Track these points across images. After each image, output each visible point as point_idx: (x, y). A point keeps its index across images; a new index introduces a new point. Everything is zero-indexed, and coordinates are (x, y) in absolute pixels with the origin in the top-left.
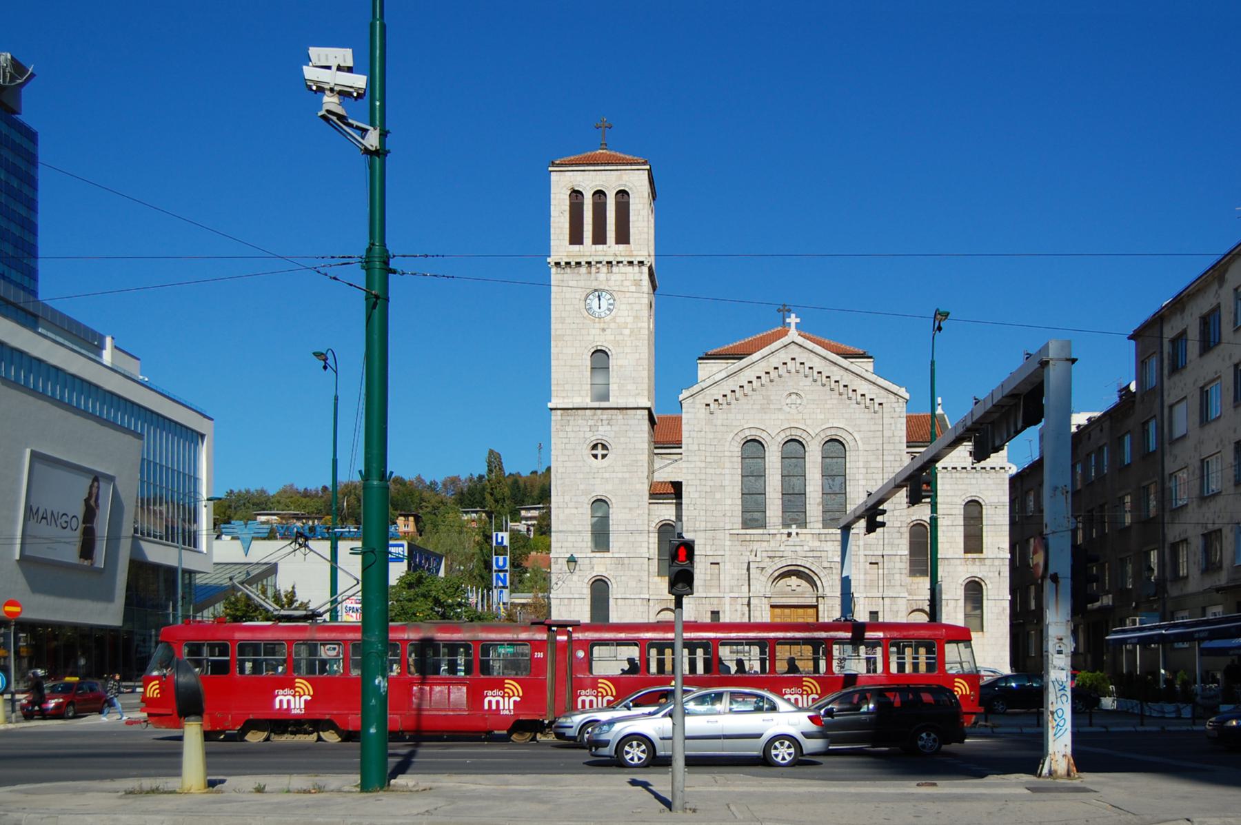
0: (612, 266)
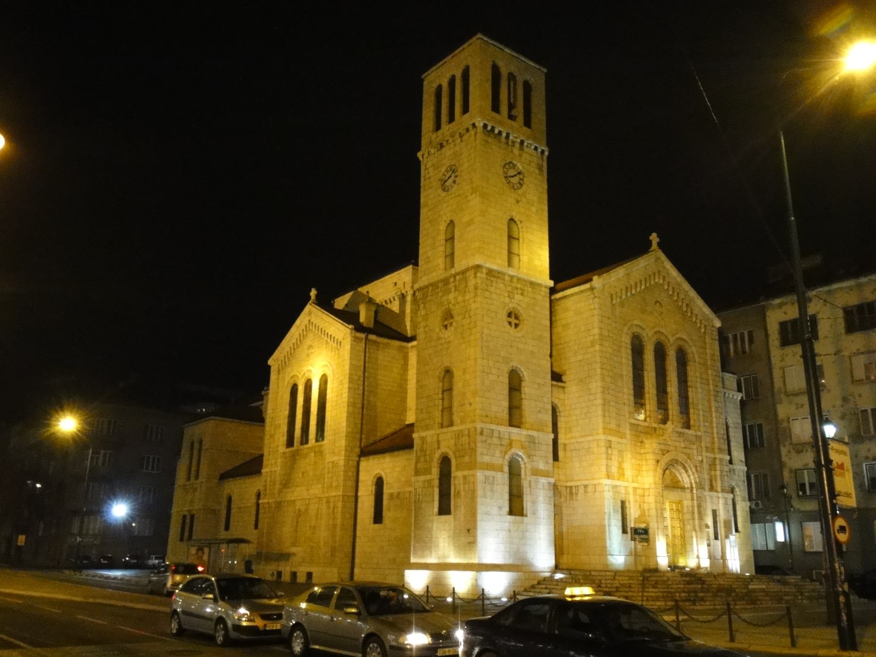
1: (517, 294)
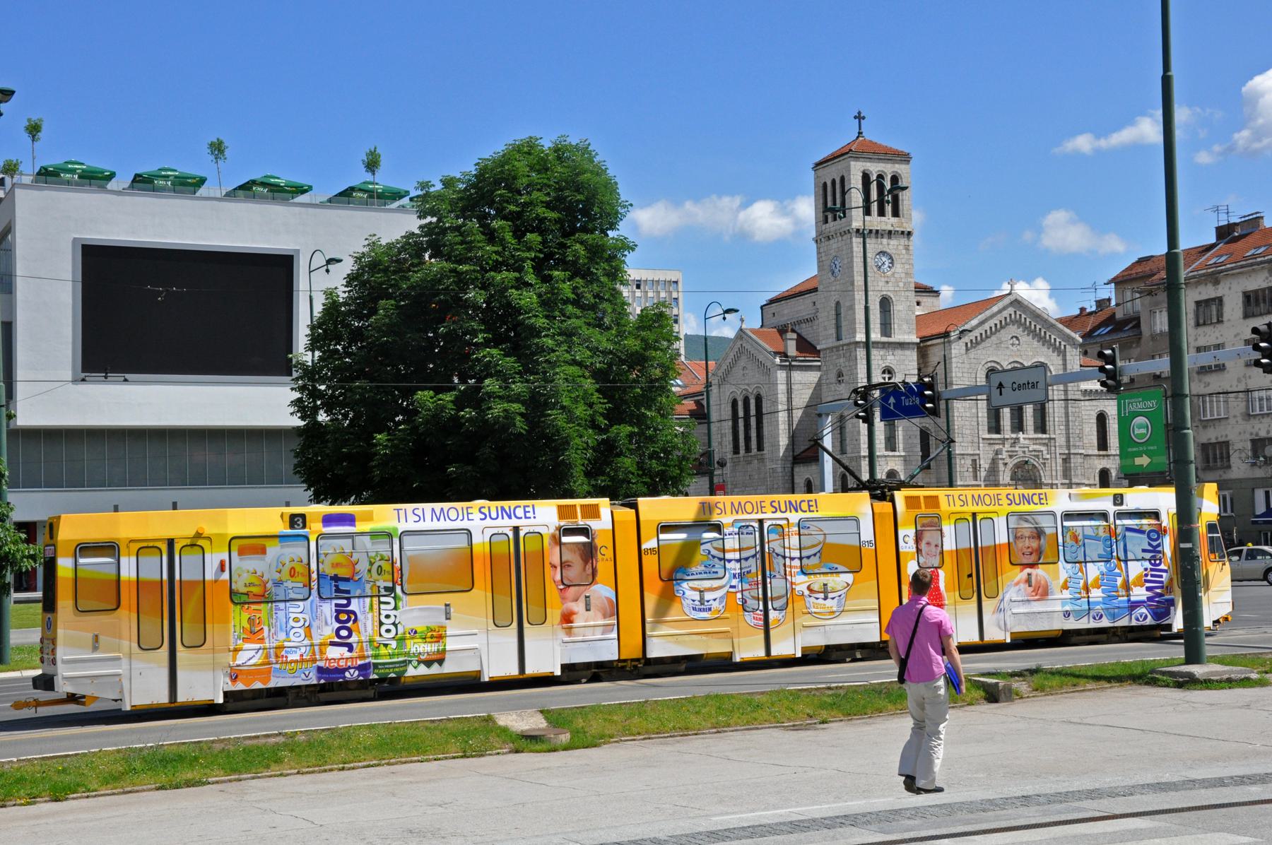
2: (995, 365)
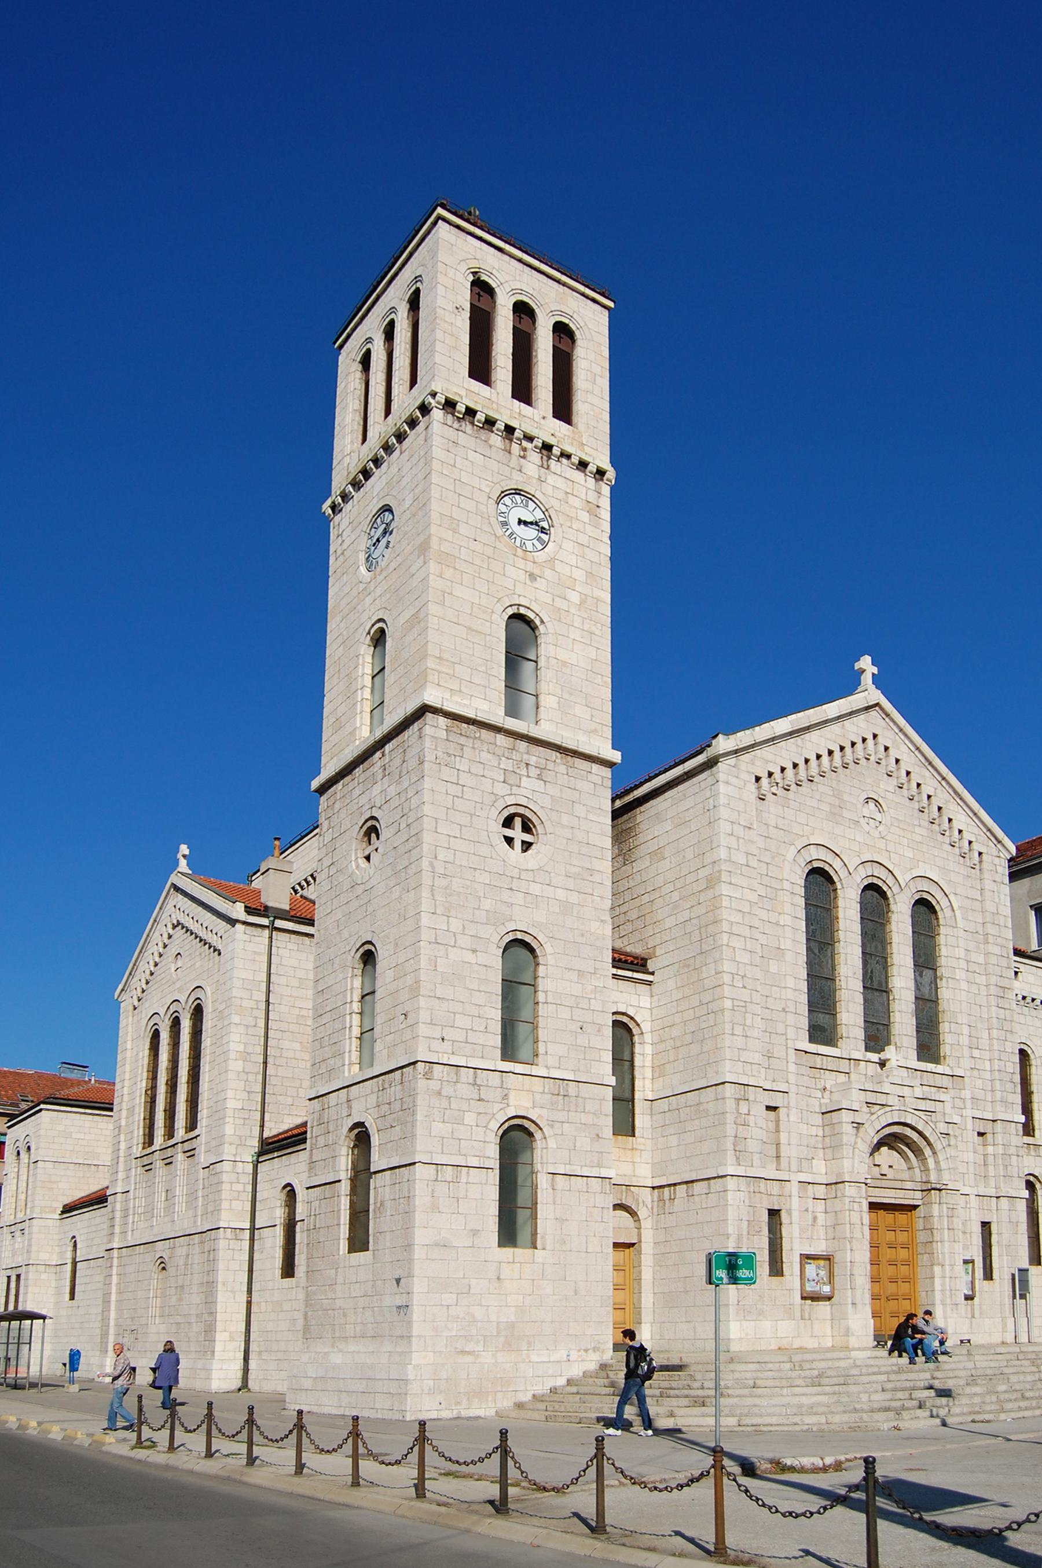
0: (549, 458)
1: (528, 776)
2: (829, 857)
